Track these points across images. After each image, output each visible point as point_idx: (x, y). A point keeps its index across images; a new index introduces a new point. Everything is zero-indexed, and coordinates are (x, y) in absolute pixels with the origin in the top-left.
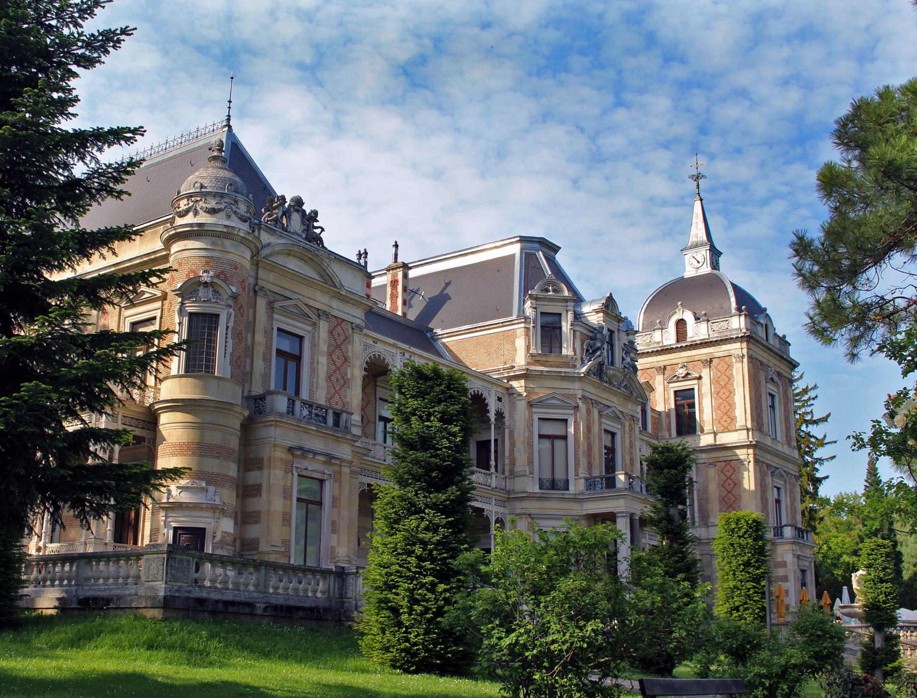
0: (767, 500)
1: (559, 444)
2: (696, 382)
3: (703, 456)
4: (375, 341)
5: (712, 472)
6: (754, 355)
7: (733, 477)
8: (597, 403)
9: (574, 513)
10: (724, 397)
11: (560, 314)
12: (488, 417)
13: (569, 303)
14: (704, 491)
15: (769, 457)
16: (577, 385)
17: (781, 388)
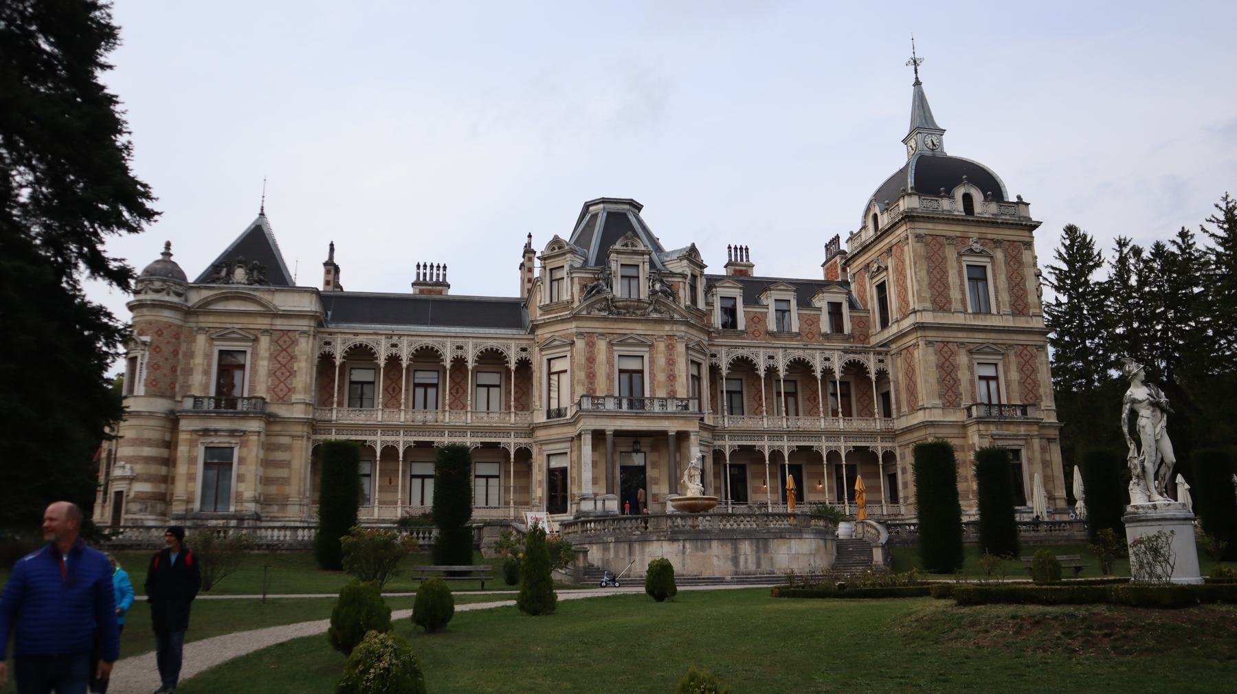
0: (956, 381)
1: (563, 376)
2: (885, 273)
3: (893, 346)
4: (356, 334)
5: (899, 361)
6: (922, 232)
7: (912, 364)
8: (602, 334)
9: (570, 435)
10: (901, 282)
11: (563, 266)
12: (507, 367)
13: (567, 255)
14: (896, 383)
15: (960, 334)
16: (574, 324)
17: (999, 255)
